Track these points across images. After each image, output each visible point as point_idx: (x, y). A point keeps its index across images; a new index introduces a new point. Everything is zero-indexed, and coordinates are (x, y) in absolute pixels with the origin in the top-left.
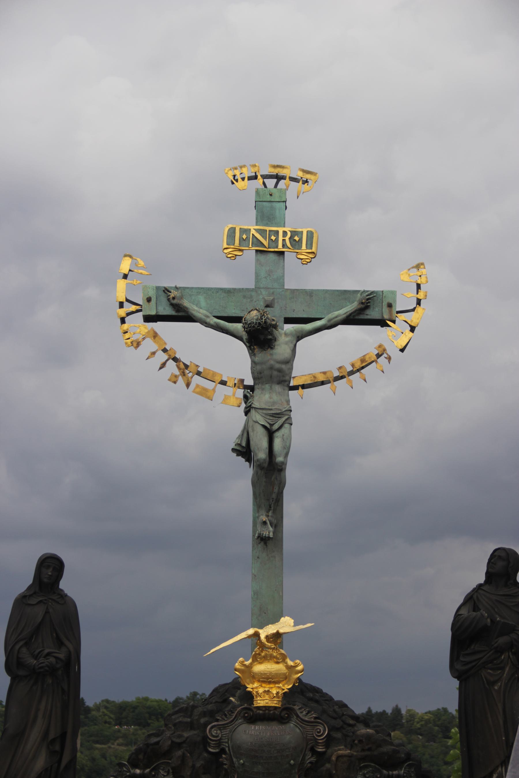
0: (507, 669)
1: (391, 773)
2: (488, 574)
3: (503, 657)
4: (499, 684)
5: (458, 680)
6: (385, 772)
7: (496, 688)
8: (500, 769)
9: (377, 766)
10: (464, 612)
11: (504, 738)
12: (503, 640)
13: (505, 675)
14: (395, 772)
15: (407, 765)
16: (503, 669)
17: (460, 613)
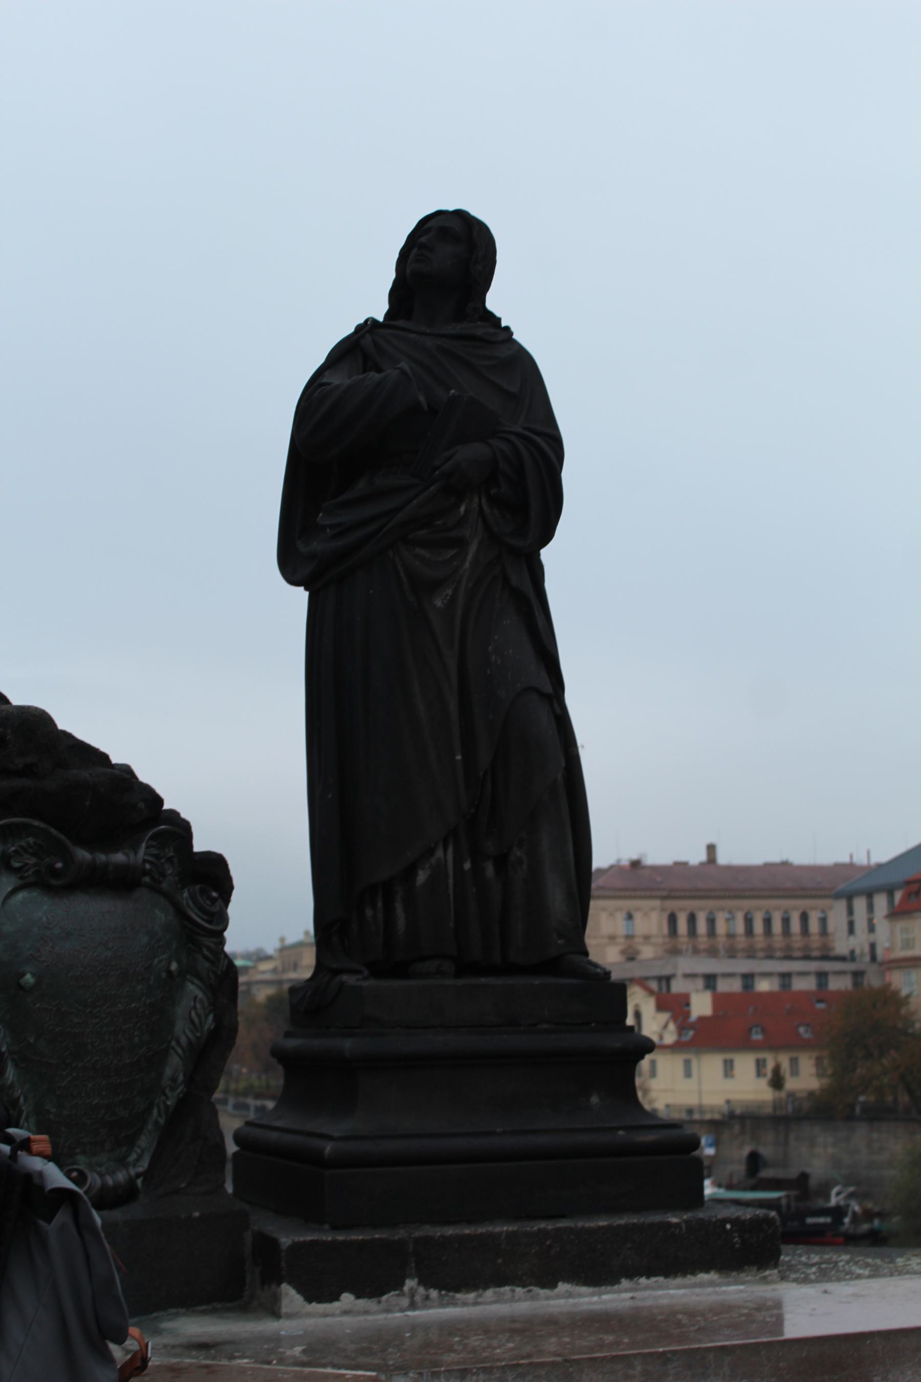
0: (473, 549)
1: (102, 857)
2: (402, 293)
3: (462, 509)
4: (449, 592)
5: (306, 589)
6: (83, 855)
7: (439, 603)
8: (439, 853)
9: (54, 831)
10: (335, 379)
11: (459, 757)
12: (470, 453)
13: (467, 565)
14: (119, 857)
15: (153, 838)
16: (461, 544)
17: (324, 380)
